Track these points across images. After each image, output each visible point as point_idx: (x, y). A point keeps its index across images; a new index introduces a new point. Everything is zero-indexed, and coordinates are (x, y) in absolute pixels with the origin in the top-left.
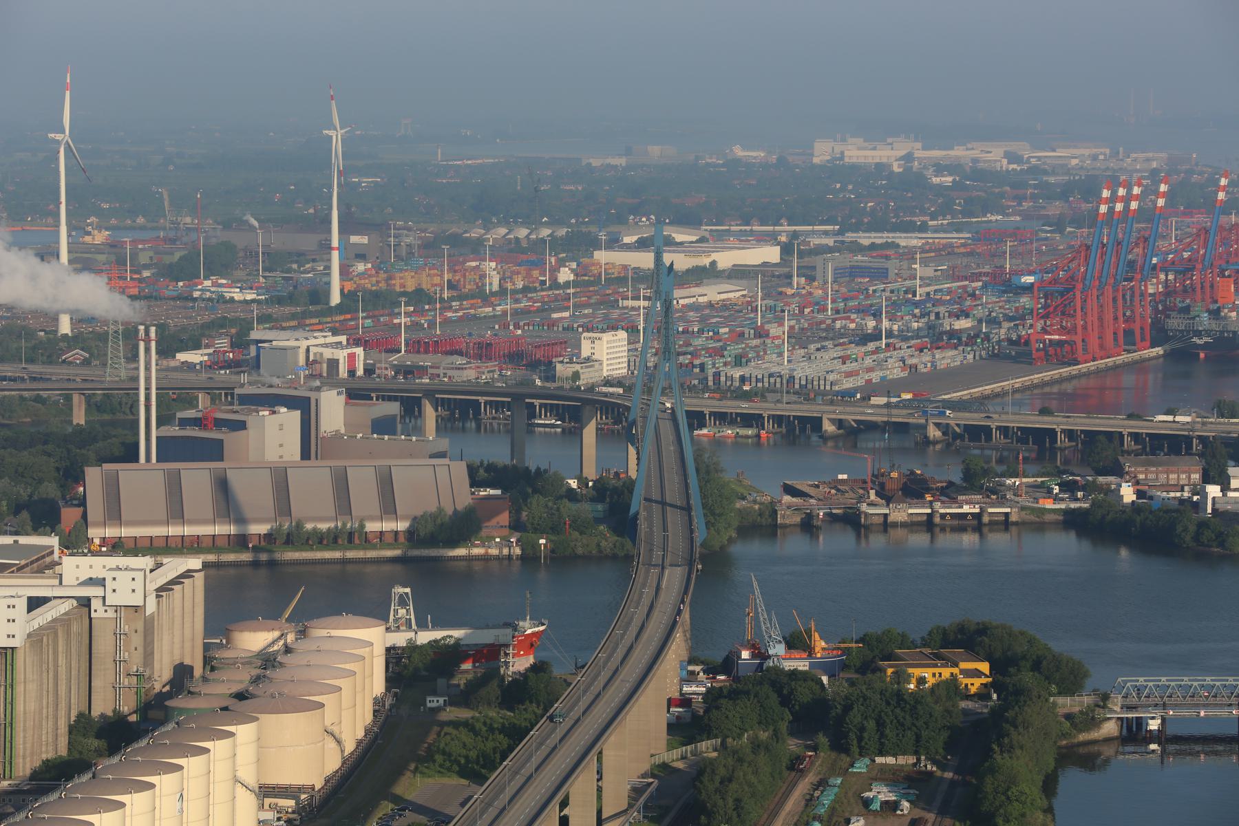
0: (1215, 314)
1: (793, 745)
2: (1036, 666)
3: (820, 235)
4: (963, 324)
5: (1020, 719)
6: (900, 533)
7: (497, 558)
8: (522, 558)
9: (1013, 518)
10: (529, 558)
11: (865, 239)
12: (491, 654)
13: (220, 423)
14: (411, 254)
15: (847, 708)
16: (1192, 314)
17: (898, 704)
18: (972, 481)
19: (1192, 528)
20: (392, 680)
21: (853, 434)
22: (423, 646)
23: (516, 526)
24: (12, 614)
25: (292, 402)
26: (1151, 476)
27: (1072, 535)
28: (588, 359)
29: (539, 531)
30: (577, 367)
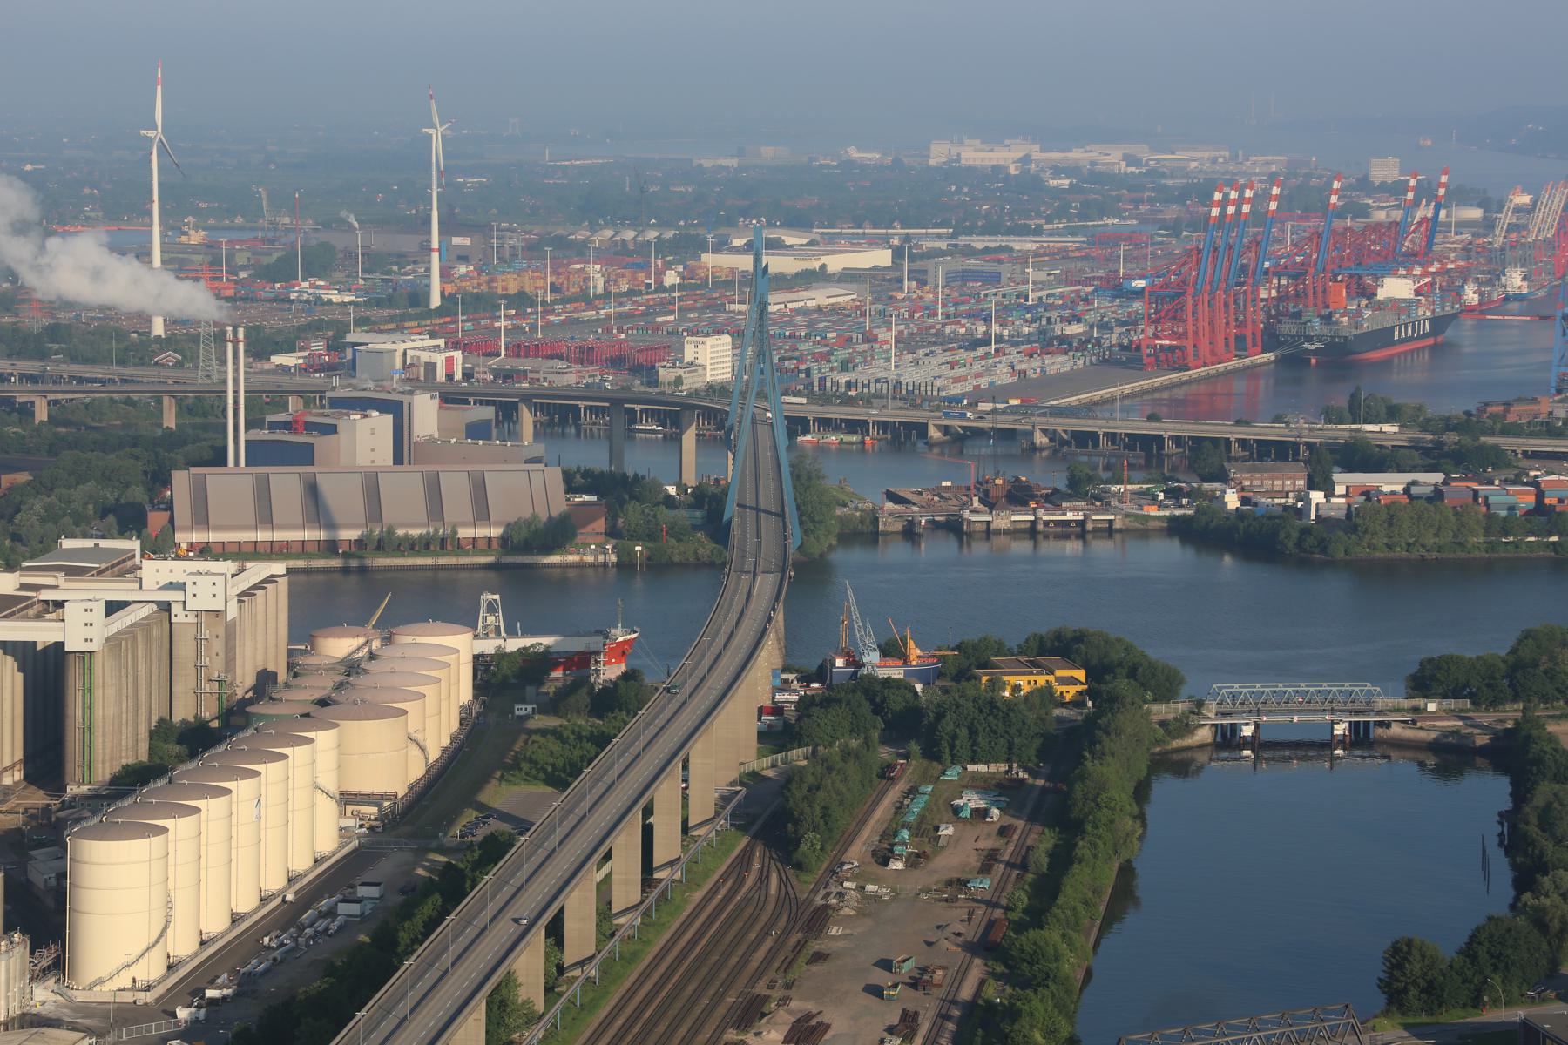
0: (1327, 319)
1: (885, 753)
2: (1132, 673)
3: (933, 239)
4: (1074, 329)
5: (1113, 725)
6: (1003, 539)
7: (593, 565)
8: (618, 565)
9: (1117, 525)
10: (625, 566)
11: (979, 243)
12: (581, 662)
13: (310, 427)
14: (514, 256)
15: (940, 716)
16: (1304, 319)
17: (991, 712)
18: (1077, 488)
19: (1295, 535)
20: (480, 687)
21: (959, 440)
22: (511, 653)
23: (612, 533)
24: (89, 617)
25: (383, 406)
26: (1255, 483)
27: (1176, 543)
28: (691, 364)
29: (635, 537)
30: (680, 372)
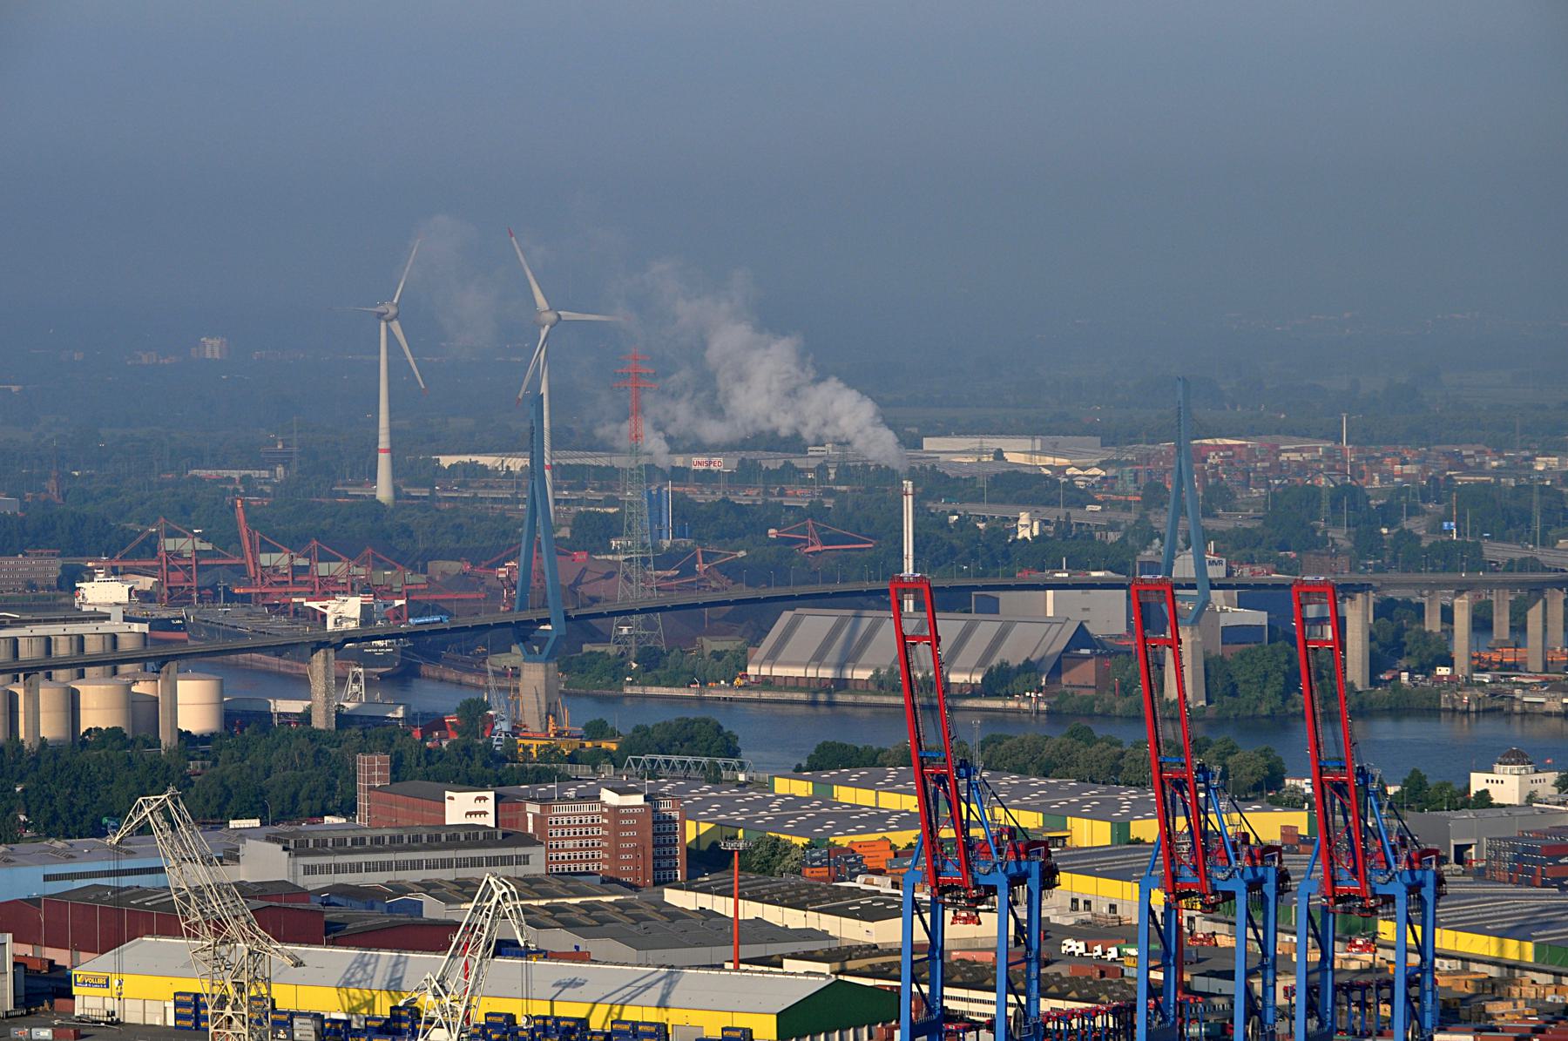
7: (1026, 711)
